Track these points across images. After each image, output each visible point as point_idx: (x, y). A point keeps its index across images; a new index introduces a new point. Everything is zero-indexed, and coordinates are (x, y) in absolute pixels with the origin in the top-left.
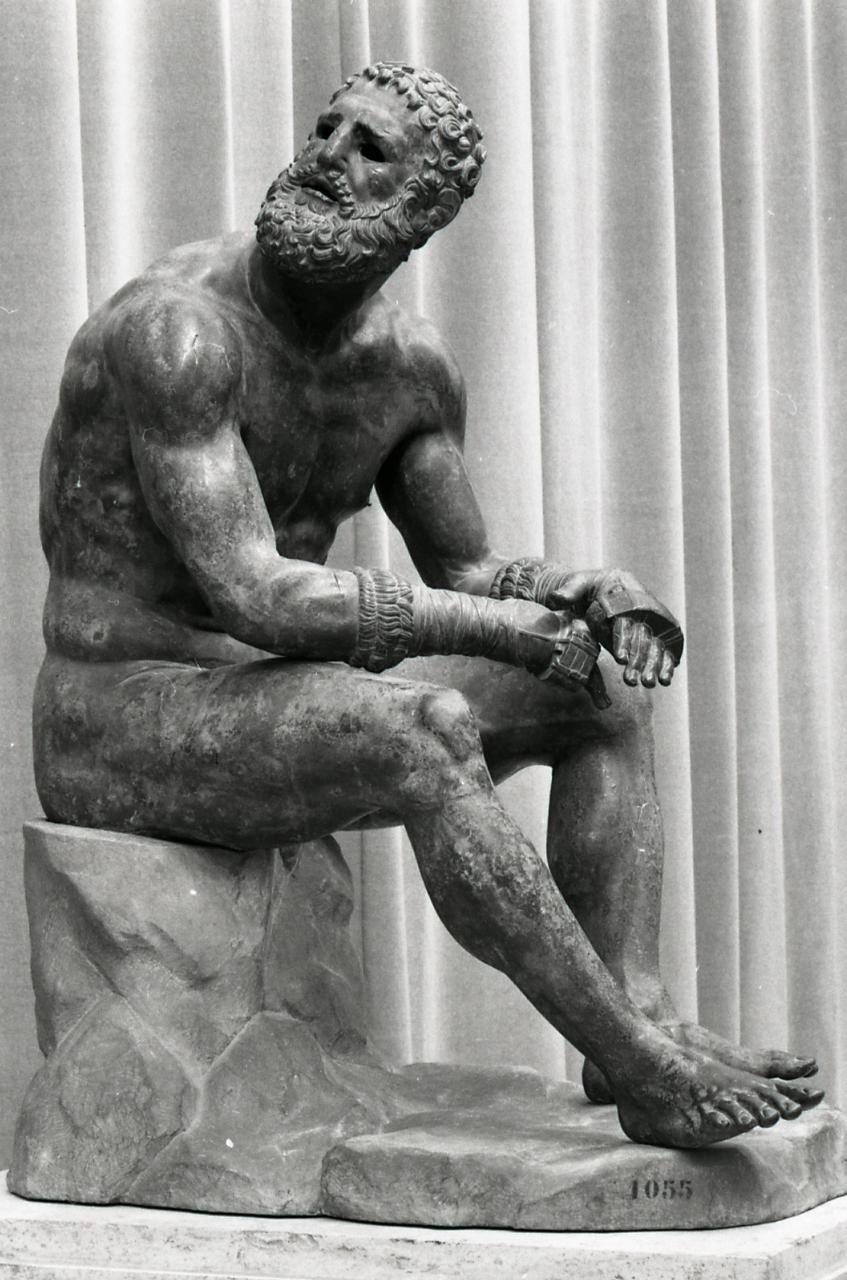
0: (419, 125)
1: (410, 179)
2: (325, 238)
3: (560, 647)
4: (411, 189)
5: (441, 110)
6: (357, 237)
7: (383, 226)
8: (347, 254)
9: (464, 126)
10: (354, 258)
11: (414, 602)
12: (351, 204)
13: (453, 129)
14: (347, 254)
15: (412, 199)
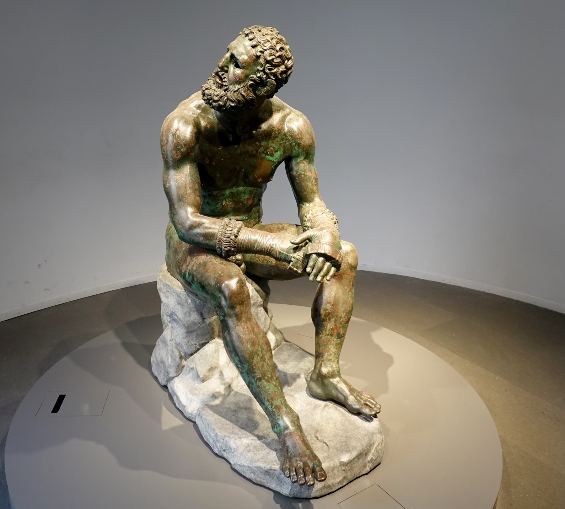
0: (255, 55)
1: (251, 76)
2: (216, 98)
3: (293, 259)
4: (251, 80)
5: (265, 48)
6: (228, 99)
7: (239, 95)
8: (225, 104)
9: (278, 54)
10: (228, 106)
11: (238, 237)
12: (226, 86)
13: (271, 55)
14: (225, 104)
15: (251, 84)
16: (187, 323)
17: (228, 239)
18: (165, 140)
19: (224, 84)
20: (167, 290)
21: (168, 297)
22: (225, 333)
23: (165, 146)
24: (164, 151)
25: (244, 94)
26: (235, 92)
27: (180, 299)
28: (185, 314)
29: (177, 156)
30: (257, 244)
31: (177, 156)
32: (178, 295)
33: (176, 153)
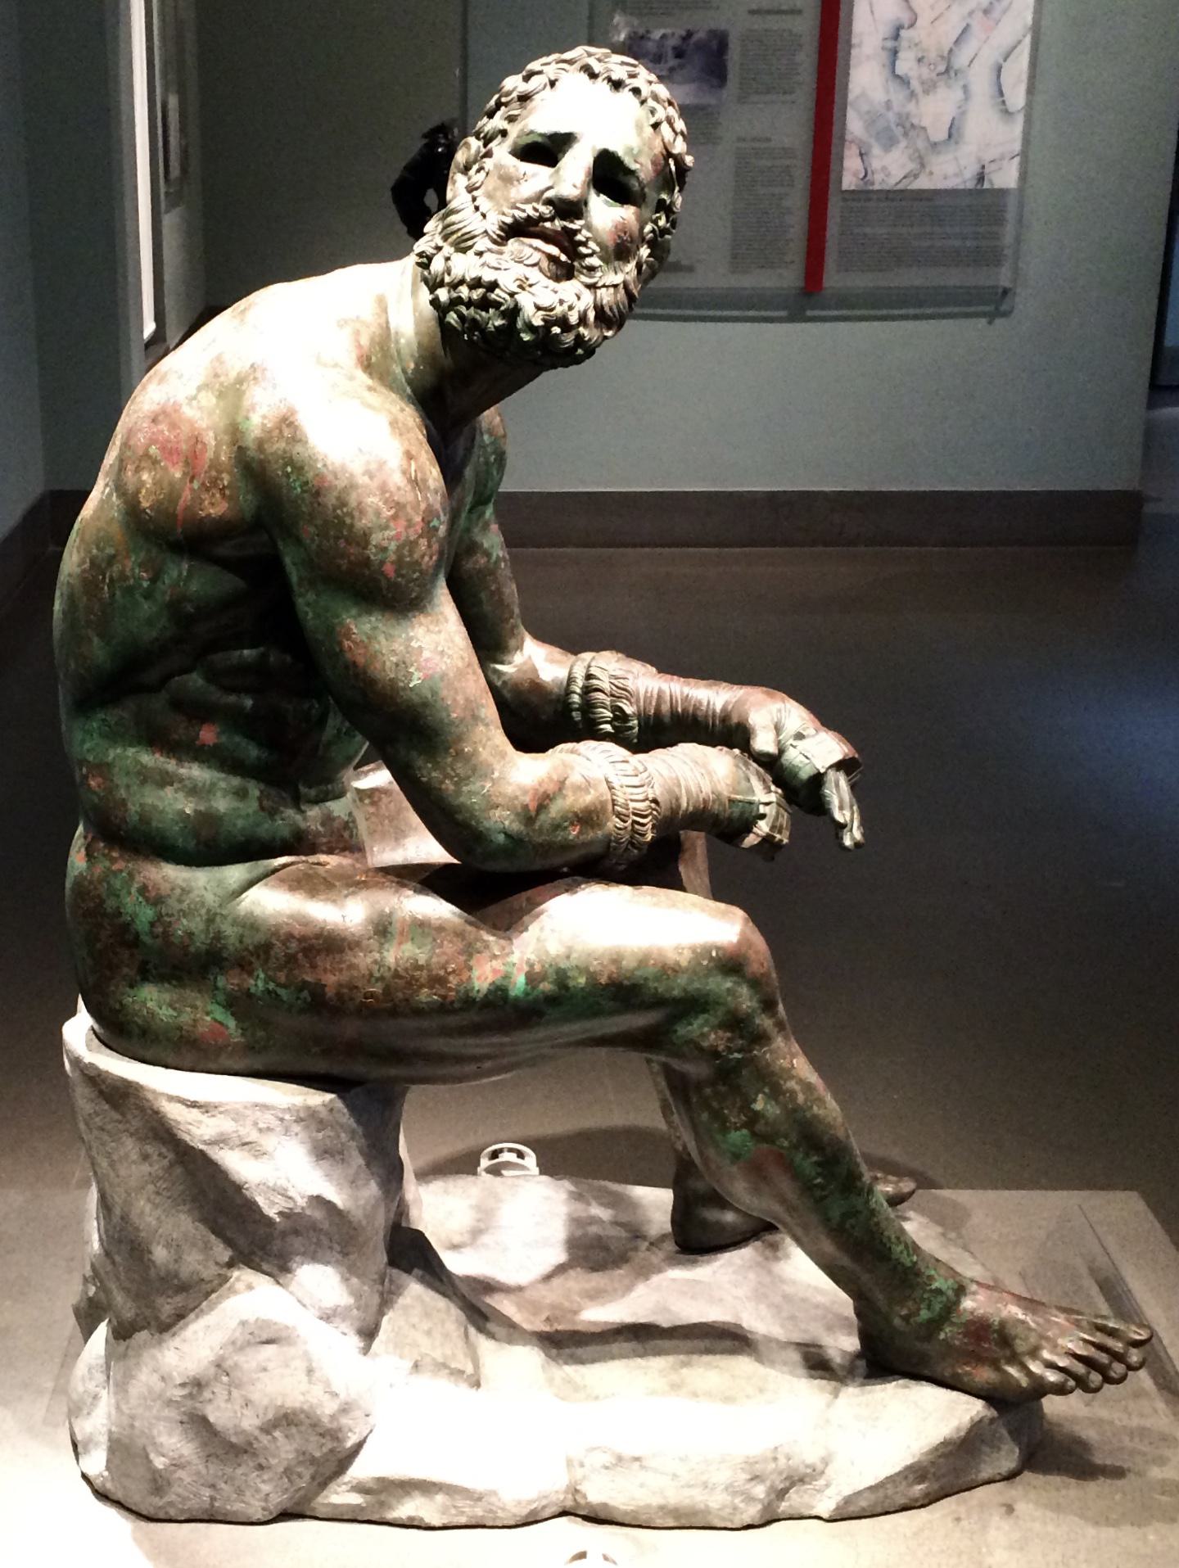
16: (364, 1209)
17: (647, 803)
18: (380, 504)
19: (594, 261)
20: (261, 1125)
21: (258, 1153)
22: (755, 1101)
23: (386, 527)
24: (384, 549)
25: (635, 292)
26: (615, 286)
27: (332, 1134)
28: (353, 1182)
29: (431, 558)
30: (684, 791)
31: (431, 558)
32: (321, 1121)
33: (429, 546)
